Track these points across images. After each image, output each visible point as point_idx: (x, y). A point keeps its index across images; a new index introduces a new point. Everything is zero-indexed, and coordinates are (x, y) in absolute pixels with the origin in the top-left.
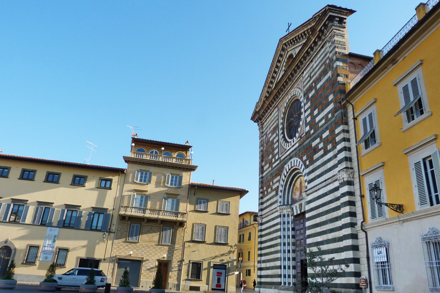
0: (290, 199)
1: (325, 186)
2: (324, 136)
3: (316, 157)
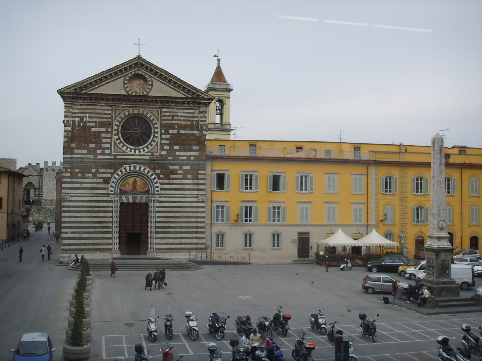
0: (118, 190)
1: (181, 197)
2: (184, 167)
3: (172, 176)
